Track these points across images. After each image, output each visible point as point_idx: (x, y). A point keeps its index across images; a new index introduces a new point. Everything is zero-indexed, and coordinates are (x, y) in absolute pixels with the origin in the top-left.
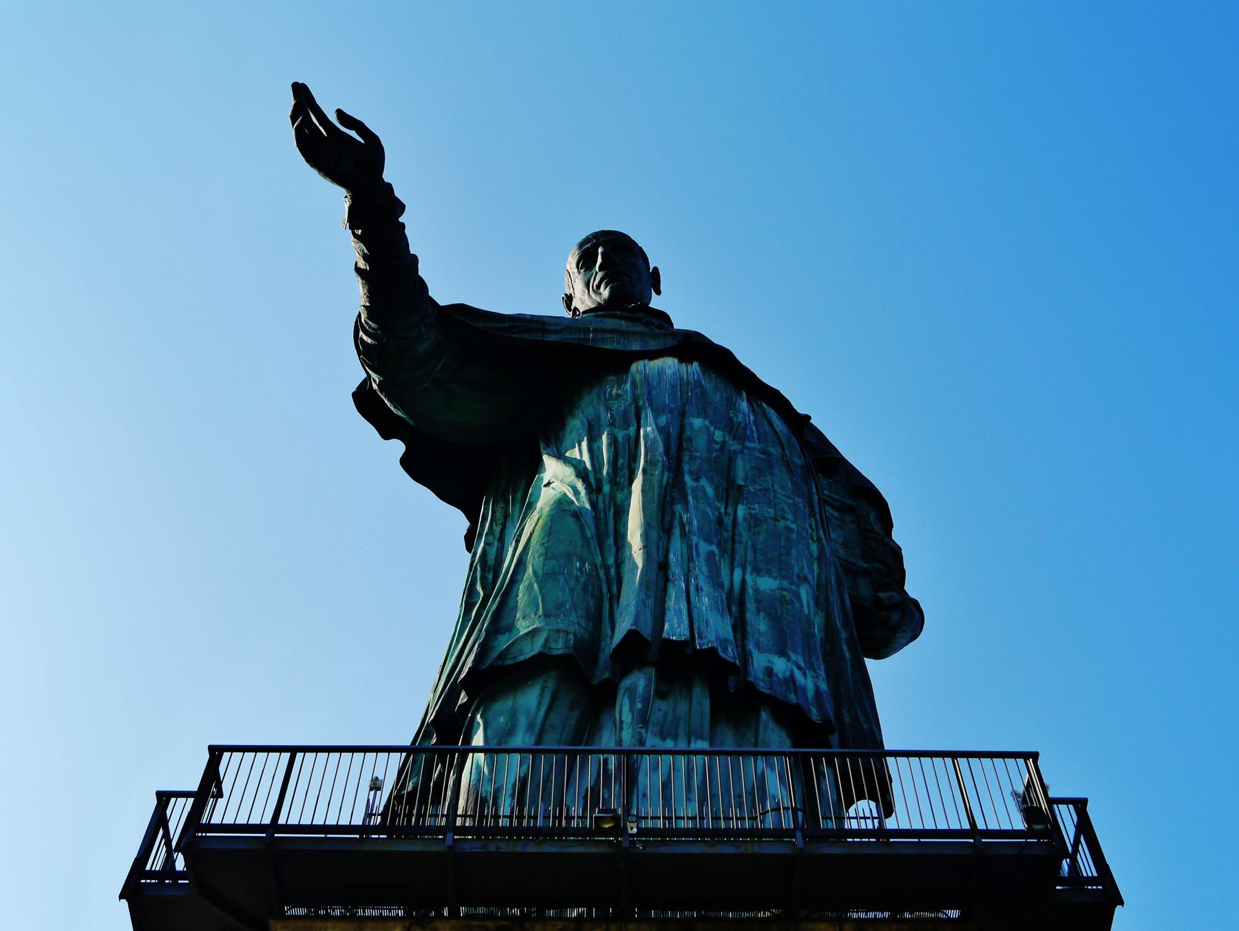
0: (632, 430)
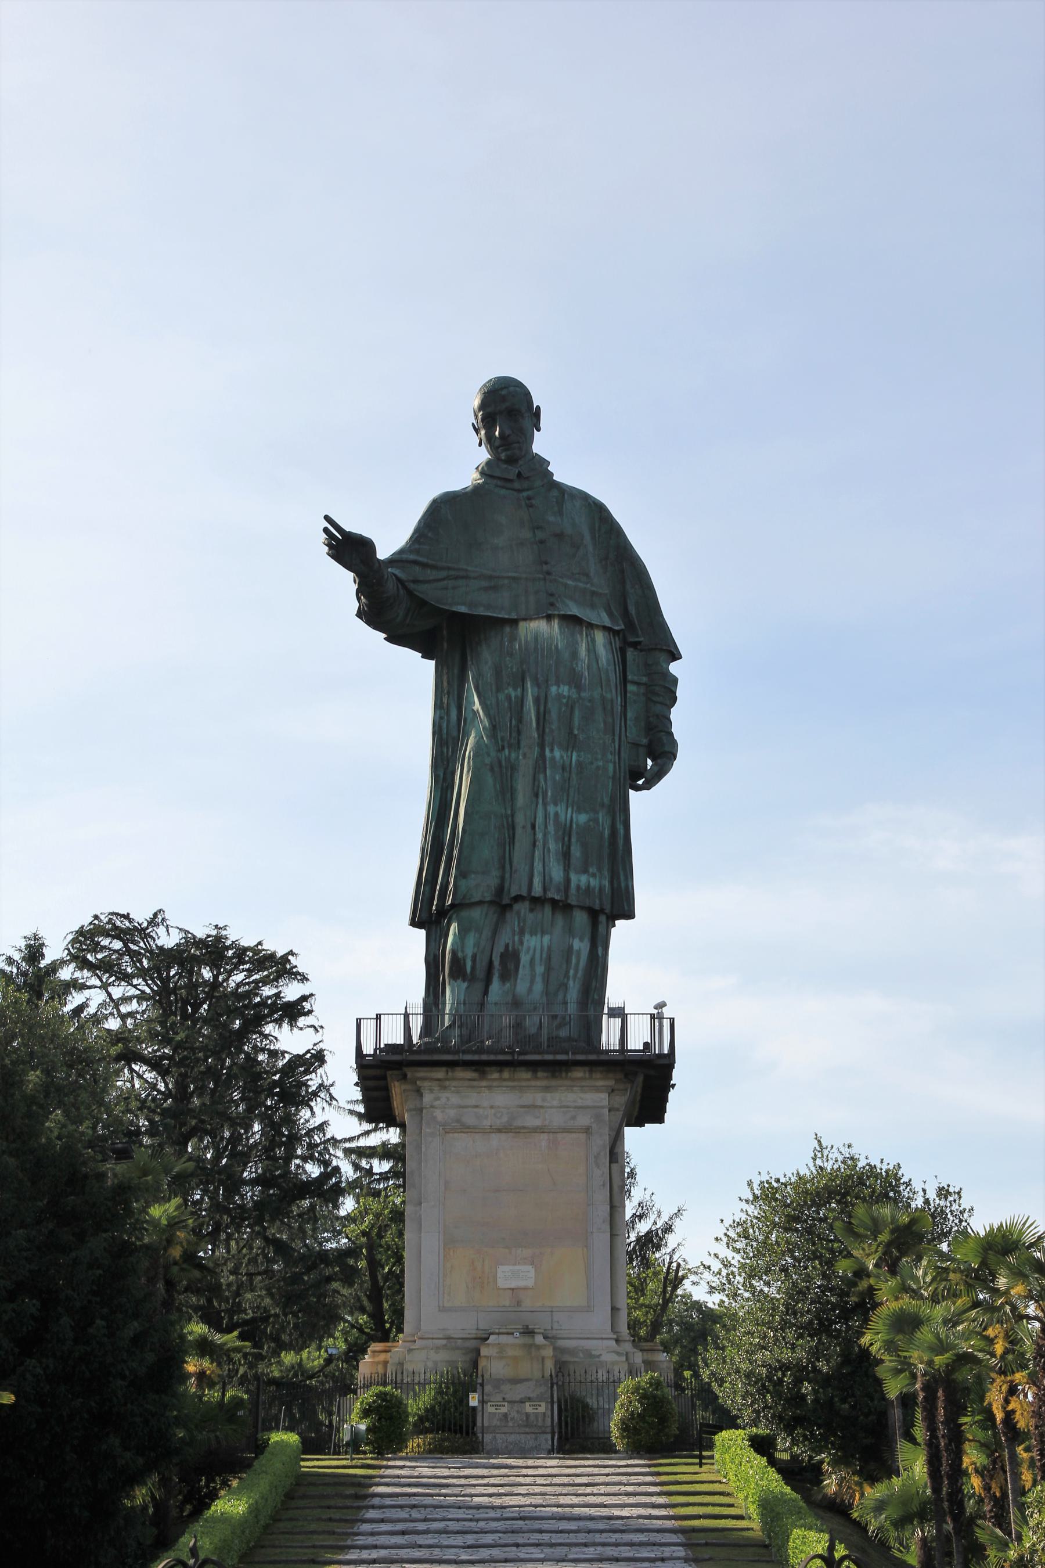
0: (519, 690)
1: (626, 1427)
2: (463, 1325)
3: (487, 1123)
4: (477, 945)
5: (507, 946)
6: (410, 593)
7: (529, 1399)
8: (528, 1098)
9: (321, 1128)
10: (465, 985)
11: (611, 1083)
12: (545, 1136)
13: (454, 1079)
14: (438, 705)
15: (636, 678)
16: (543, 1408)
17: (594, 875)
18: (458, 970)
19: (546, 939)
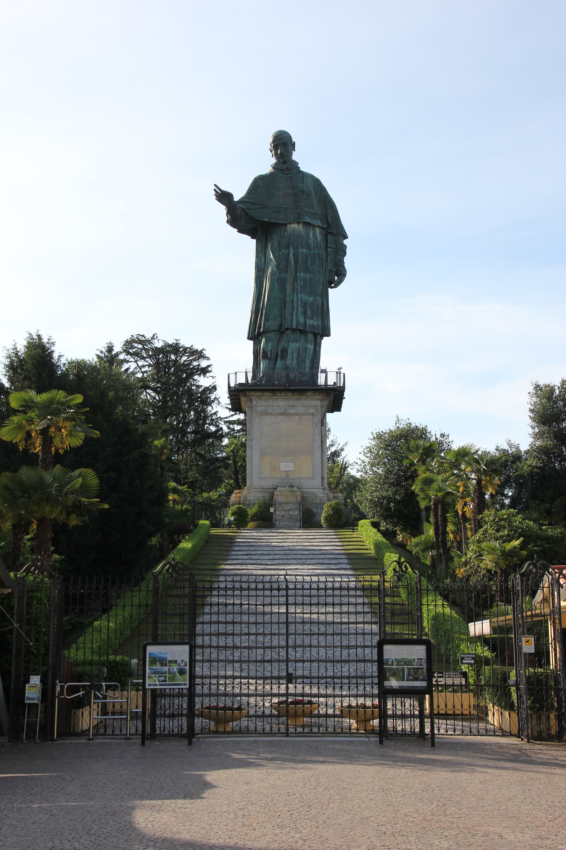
1: (327, 519)
2: (268, 484)
3: (276, 412)
4: (272, 346)
5: (283, 347)
6: (246, 214)
7: (292, 510)
8: (292, 402)
9: (215, 413)
10: (268, 361)
11: (321, 397)
12: (297, 416)
13: (264, 396)
14: (257, 256)
15: (331, 246)
16: (297, 512)
17: (315, 320)
18: (265, 356)
19: (298, 344)
